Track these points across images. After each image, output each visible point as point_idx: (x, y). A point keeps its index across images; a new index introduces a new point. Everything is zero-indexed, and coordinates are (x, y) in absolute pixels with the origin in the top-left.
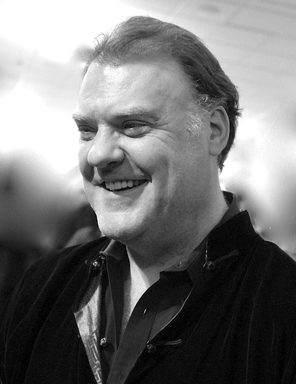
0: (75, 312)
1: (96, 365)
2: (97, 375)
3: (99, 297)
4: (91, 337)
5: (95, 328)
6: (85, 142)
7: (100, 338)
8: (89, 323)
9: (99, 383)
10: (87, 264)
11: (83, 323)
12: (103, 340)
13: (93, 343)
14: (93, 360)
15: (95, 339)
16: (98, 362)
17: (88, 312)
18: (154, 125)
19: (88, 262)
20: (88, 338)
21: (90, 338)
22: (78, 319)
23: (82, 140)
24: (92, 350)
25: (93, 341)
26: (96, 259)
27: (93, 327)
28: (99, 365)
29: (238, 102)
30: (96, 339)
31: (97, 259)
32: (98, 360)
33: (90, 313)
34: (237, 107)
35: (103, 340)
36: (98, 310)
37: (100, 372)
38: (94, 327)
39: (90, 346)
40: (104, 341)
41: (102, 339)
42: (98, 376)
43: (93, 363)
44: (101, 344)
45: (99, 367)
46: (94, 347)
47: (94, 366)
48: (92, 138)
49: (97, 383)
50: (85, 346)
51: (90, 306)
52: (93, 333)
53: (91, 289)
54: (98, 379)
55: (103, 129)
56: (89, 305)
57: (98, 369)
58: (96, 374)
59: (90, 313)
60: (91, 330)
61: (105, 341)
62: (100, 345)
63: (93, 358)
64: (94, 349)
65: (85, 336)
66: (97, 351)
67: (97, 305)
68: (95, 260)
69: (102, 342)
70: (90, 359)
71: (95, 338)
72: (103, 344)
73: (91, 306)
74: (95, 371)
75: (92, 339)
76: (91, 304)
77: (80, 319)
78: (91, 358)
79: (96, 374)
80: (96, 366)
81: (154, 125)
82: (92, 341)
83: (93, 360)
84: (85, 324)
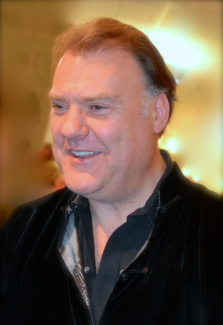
0: (59, 248)
1: (83, 287)
2: (84, 296)
3: (77, 235)
4: (76, 267)
5: (78, 259)
6: (57, 116)
7: (83, 266)
8: (72, 256)
9: (87, 301)
10: (63, 210)
11: (67, 256)
12: (87, 268)
13: (79, 271)
14: (80, 284)
15: (80, 268)
16: (84, 285)
17: (69, 247)
18: (115, 108)
19: (63, 209)
20: (73, 268)
21: (75, 267)
22: (62, 254)
23: (55, 114)
24: (78, 276)
25: (79, 269)
26: (68, 206)
27: (77, 259)
28: (85, 287)
29: (176, 89)
30: (81, 268)
31: (69, 206)
32: (84, 283)
33: (71, 248)
34: (175, 93)
35: (87, 268)
36: (78, 245)
37: (87, 293)
38: (78, 258)
39: (76, 273)
40: (88, 269)
41: (86, 268)
42: (86, 296)
43: (81, 287)
44: (85, 271)
45: (86, 289)
46: (80, 274)
47: (81, 289)
48: (64, 114)
49: (85, 301)
50: (72, 273)
51: (71, 242)
52: (78, 263)
53: (68, 229)
54: (85, 298)
55: (74, 109)
56: (69, 242)
57: (85, 291)
58: (83, 294)
59: (71, 248)
60: (75, 261)
61: (89, 270)
62: (84, 272)
63: (80, 283)
64: (81, 276)
65: (70, 266)
66: (83, 277)
67: (77, 241)
68: (68, 207)
69: (87, 269)
70: (77, 284)
71: (80, 266)
72: (87, 272)
73: (71, 242)
74: (83, 293)
75: (78, 268)
76: (71, 241)
77: (64, 253)
78: (79, 283)
79: (83, 294)
80: (83, 289)
81: (115, 108)
82: (77, 270)
83: (80, 284)
84: (69, 257)
